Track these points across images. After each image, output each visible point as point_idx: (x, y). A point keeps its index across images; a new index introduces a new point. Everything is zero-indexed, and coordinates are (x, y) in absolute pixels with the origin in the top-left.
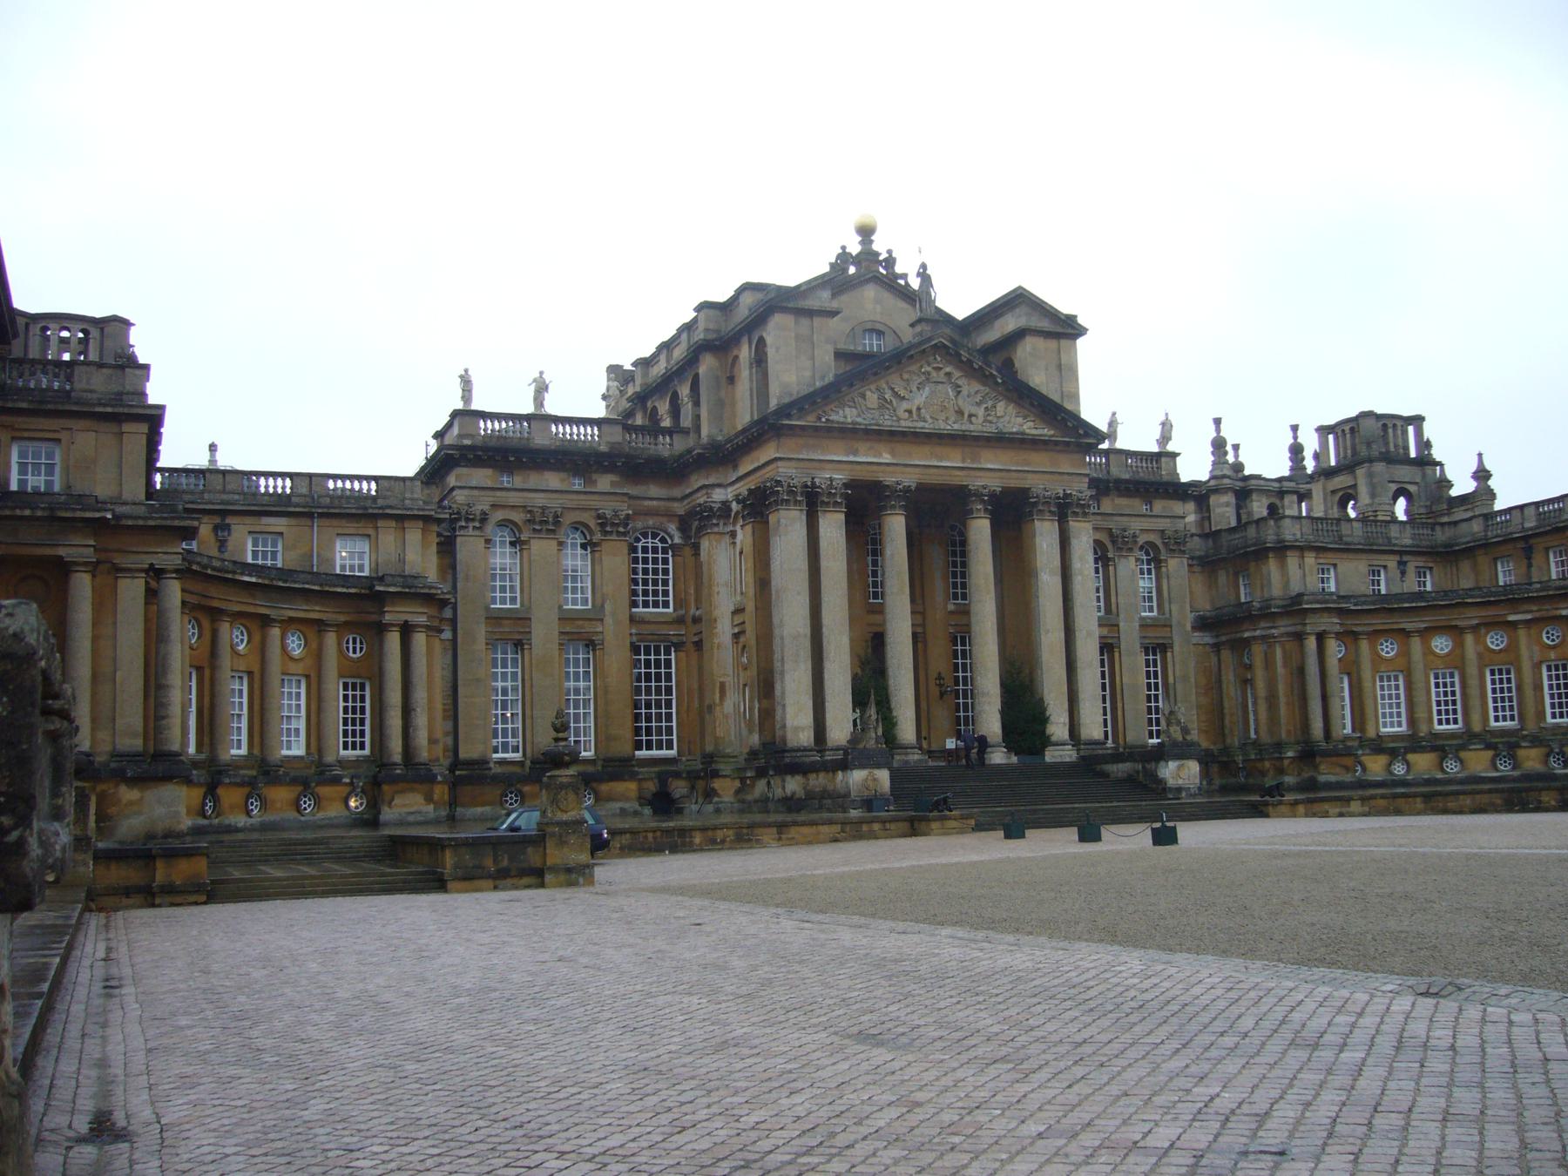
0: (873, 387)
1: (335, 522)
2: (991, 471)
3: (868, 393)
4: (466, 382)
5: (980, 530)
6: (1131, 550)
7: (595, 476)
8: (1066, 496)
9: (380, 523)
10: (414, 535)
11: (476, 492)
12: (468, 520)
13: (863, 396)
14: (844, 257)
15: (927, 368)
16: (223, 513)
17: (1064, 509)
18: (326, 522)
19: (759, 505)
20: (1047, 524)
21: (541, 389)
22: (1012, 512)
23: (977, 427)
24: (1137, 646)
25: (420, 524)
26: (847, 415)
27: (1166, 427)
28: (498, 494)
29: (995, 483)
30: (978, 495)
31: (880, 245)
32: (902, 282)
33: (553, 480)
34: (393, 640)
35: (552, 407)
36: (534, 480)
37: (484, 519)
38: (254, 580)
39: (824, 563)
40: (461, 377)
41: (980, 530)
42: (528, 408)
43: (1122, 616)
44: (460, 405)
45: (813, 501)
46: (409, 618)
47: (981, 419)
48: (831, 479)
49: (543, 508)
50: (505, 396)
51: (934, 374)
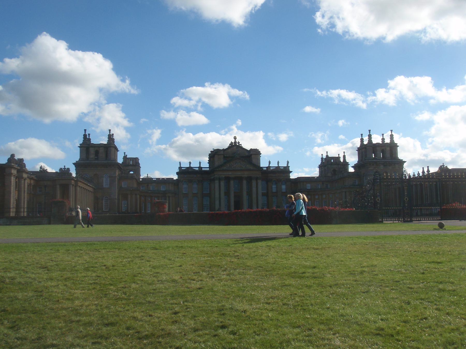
2: (246, 174)
4: (180, 163)
5: (245, 182)
14: (232, 143)
17: (257, 179)
19: (214, 180)
22: (249, 179)
26: (225, 168)
27: (288, 162)
31: (237, 141)
34: (168, 198)
35: (192, 166)
41: (245, 182)
42: (188, 166)
45: (220, 179)
50: (185, 165)
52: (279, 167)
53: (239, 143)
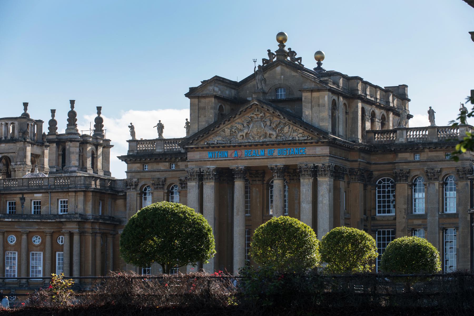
0: (229, 126)
1: (56, 194)
3: (226, 129)
4: (132, 127)
5: (277, 183)
6: (437, 179)
7: (180, 164)
8: (316, 167)
9: (70, 194)
10: (81, 197)
11: (134, 174)
12: (130, 186)
13: (224, 131)
15: (252, 115)
16: (23, 194)
17: (315, 172)
18: (53, 194)
20: (306, 181)
21: (160, 127)
23: (273, 138)
24: (437, 228)
25: (83, 193)
26: (216, 139)
28: (142, 174)
29: (280, 163)
30: (272, 169)
32: (297, 62)
33: (163, 166)
36: (155, 166)
37: (136, 185)
38: (10, 220)
39: (205, 204)
40: (129, 127)
41: (277, 183)
43: (429, 215)
44: (131, 138)
45: (201, 177)
46: (71, 230)
47: (275, 136)
48: (208, 169)
49: (159, 179)
50: (147, 133)
51: (255, 117)
52: (433, 128)
53: (292, 53)
